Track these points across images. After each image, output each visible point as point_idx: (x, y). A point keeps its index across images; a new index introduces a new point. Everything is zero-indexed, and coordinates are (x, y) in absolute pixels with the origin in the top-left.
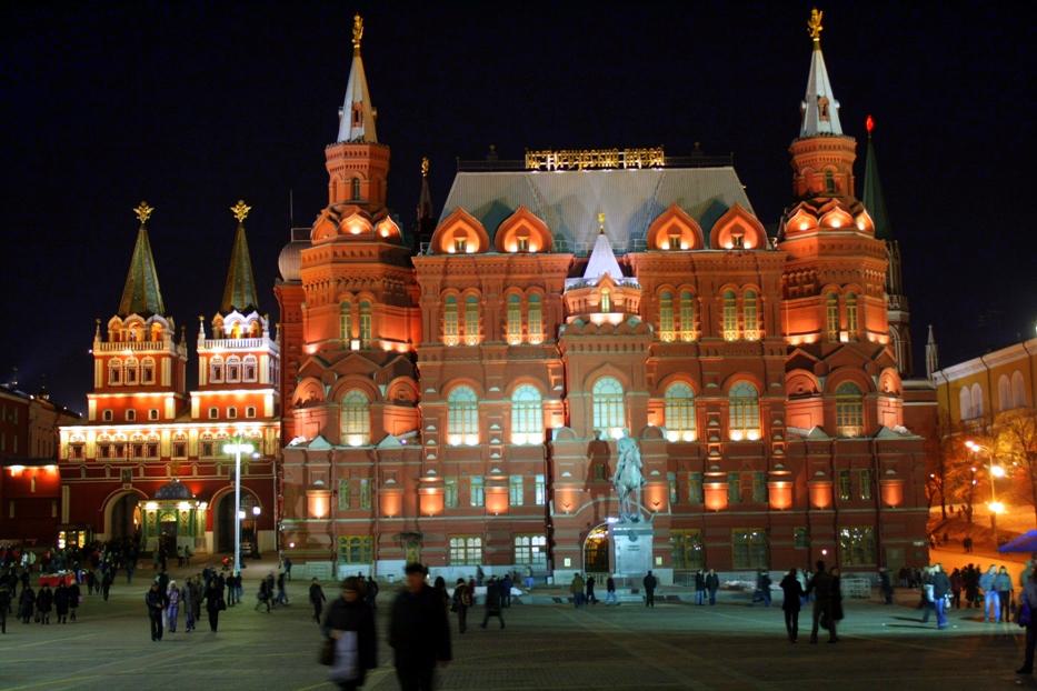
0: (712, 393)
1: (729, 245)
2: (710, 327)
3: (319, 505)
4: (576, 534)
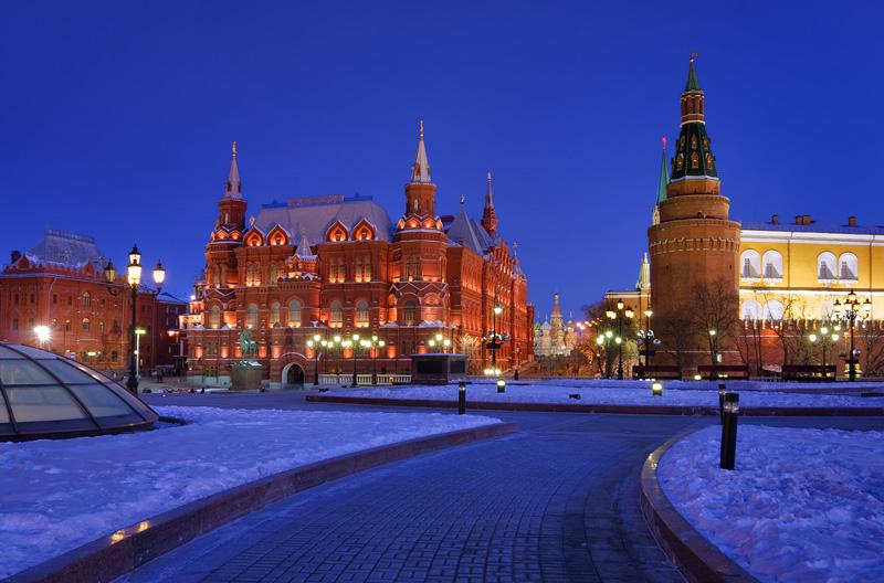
0: (349, 306)
1: (360, 238)
2: (349, 277)
3: (199, 354)
4: (279, 367)
